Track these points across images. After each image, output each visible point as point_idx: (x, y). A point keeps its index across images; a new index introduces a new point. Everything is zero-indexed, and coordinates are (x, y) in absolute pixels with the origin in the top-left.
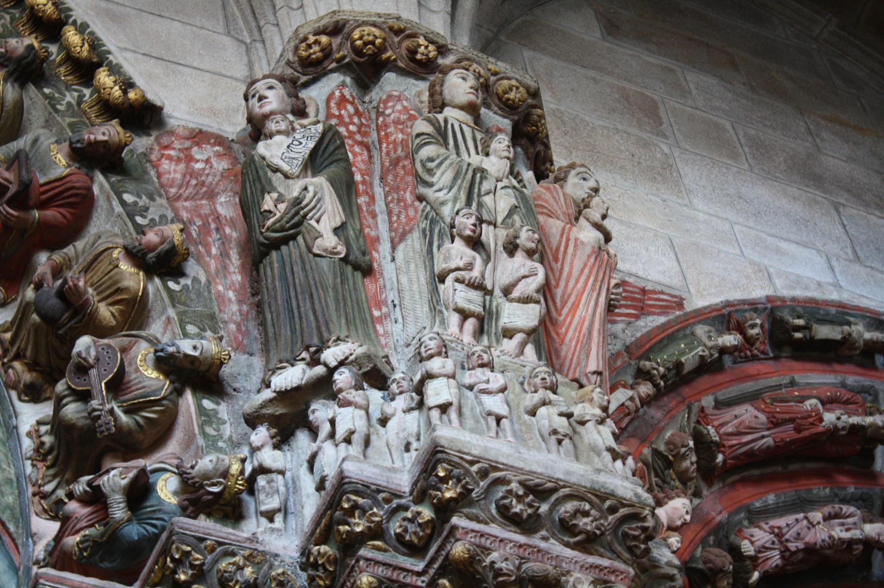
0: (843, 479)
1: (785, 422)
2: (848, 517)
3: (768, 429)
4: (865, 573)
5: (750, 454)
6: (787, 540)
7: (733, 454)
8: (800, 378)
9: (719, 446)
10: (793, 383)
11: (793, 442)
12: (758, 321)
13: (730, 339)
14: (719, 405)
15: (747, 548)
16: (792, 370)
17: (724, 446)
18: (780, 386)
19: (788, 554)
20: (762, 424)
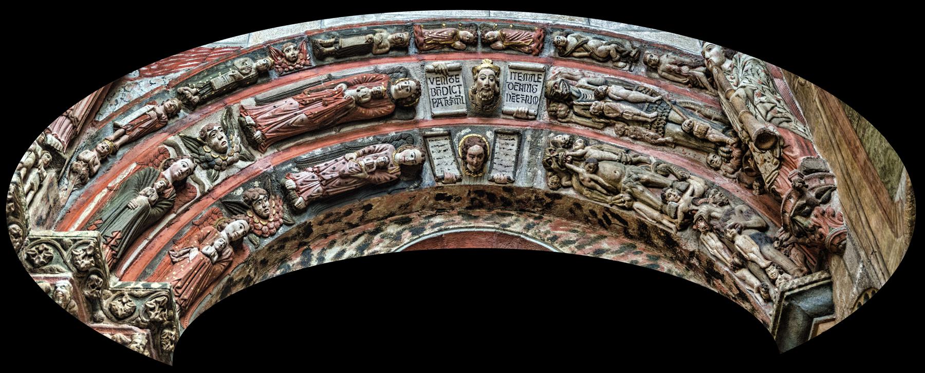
0: (388, 129)
1: (312, 102)
2: (381, 151)
3: (300, 109)
4: (416, 185)
5: (289, 127)
6: (324, 174)
7: (272, 129)
8: (333, 74)
9: (256, 126)
10: (330, 78)
11: (322, 113)
12: (292, 47)
13: (261, 62)
14: (259, 103)
15: (290, 184)
16: (330, 70)
17: (260, 126)
18: (319, 82)
19: (324, 182)
20: (295, 107)
